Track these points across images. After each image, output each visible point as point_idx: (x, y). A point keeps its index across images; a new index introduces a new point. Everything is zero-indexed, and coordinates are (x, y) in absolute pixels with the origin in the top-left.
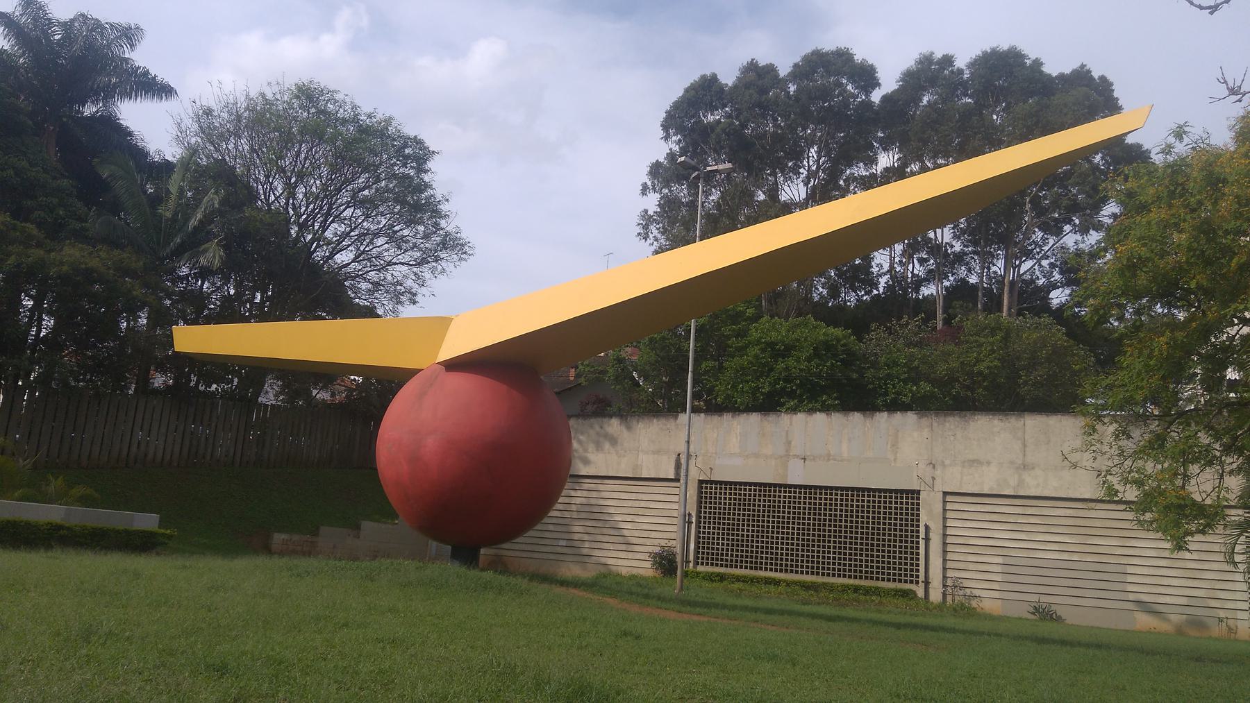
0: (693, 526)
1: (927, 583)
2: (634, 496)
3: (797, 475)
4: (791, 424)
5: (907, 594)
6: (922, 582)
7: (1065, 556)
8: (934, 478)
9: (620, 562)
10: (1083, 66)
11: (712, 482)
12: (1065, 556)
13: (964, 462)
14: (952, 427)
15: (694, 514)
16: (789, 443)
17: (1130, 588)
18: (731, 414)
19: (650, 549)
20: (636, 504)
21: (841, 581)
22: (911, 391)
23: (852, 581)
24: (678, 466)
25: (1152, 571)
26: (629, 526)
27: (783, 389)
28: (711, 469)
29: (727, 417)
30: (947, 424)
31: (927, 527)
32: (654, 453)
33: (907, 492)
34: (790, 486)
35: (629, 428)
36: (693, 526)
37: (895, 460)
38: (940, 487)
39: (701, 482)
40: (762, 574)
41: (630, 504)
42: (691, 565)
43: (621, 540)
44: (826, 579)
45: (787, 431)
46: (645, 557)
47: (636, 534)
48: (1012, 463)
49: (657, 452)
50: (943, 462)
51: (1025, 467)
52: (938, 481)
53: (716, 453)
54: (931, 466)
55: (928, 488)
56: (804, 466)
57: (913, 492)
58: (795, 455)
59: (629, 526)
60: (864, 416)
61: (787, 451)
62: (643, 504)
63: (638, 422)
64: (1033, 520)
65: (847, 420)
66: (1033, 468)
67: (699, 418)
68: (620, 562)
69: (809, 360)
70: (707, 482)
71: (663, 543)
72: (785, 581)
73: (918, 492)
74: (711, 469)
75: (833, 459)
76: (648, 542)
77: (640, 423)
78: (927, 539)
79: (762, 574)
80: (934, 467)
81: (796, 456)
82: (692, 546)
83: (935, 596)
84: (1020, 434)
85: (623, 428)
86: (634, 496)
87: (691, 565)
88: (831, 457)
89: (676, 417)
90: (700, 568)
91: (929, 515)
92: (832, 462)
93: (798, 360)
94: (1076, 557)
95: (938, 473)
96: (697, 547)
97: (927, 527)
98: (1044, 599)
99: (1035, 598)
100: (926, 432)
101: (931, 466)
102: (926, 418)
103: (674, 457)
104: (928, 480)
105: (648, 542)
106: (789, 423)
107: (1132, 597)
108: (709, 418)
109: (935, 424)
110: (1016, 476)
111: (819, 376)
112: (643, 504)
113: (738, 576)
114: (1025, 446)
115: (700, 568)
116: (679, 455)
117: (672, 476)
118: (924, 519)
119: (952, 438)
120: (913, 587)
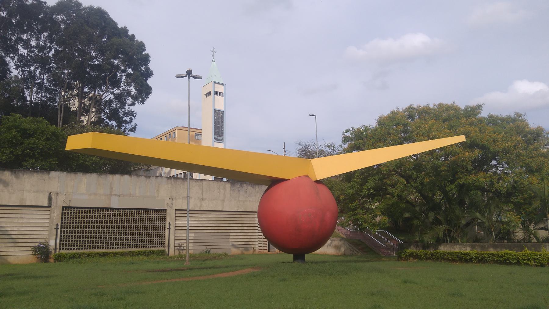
1: (169, 246)
2: (19, 216)
3: (115, 203)
4: (113, 180)
5: (164, 251)
6: (167, 246)
7: (213, 231)
8: (172, 204)
9: (10, 253)
11: (69, 207)
12: (213, 231)
13: (183, 197)
14: (179, 184)
15: (59, 224)
16: (112, 188)
17: (230, 240)
18: (82, 173)
20: (21, 220)
21: (138, 249)
22: (92, 160)
24: (50, 199)
25: (236, 234)
26: (16, 233)
28: (70, 201)
29: (80, 175)
30: (178, 183)
31: (169, 223)
32: (34, 192)
33: (161, 210)
34: (111, 209)
35: (17, 177)
36: (59, 230)
37: (158, 196)
38: (175, 207)
39: (63, 207)
40: (96, 251)
41: (16, 220)
42: (58, 250)
43: (11, 241)
45: (111, 183)
46: (30, 249)
47: (21, 237)
48: (199, 198)
49: (37, 191)
50: (176, 198)
51: (203, 199)
52: (174, 205)
53: (72, 193)
54: (172, 199)
55: (170, 208)
56: (119, 199)
57: (163, 210)
58: (115, 194)
59: (16, 233)
60: (146, 178)
61: (111, 192)
62: (25, 220)
63: (23, 175)
64: (204, 219)
65: (139, 179)
66: (205, 200)
67: (63, 174)
68: (10, 253)
69: (44, 140)
70: (66, 207)
71: (41, 240)
72: (112, 253)
73: (166, 210)
74: (70, 201)
75: (132, 196)
76: (29, 241)
77: (25, 175)
78: (169, 229)
79: (96, 251)
80: (172, 199)
81: (115, 195)
82: (58, 241)
83: (171, 253)
84: (201, 187)
85: (13, 177)
86: (19, 216)
87: (58, 250)
88: (131, 195)
89: (49, 173)
90: (62, 252)
91: (170, 219)
92: (131, 197)
93: (39, 139)
94: (216, 231)
95: (174, 201)
96: (60, 241)
97: (169, 223)
98: (208, 247)
99: (205, 247)
100: (170, 186)
101: (172, 199)
102: (170, 180)
103: (47, 195)
104: (170, 205)
105: (29, 241)
106: (112, 179)
107: (230, 243)
108: (69, 175)
109: (173, 182)
110: (200, 203)
111: (49, 149)
112: (25, 220)
113: (89, 253)
114: (203, 191)
115: (62, 252)
116: (50, 193)
117: (46, 204)
118: (168, 220)
119: (179, 188)
120: (162, 249)
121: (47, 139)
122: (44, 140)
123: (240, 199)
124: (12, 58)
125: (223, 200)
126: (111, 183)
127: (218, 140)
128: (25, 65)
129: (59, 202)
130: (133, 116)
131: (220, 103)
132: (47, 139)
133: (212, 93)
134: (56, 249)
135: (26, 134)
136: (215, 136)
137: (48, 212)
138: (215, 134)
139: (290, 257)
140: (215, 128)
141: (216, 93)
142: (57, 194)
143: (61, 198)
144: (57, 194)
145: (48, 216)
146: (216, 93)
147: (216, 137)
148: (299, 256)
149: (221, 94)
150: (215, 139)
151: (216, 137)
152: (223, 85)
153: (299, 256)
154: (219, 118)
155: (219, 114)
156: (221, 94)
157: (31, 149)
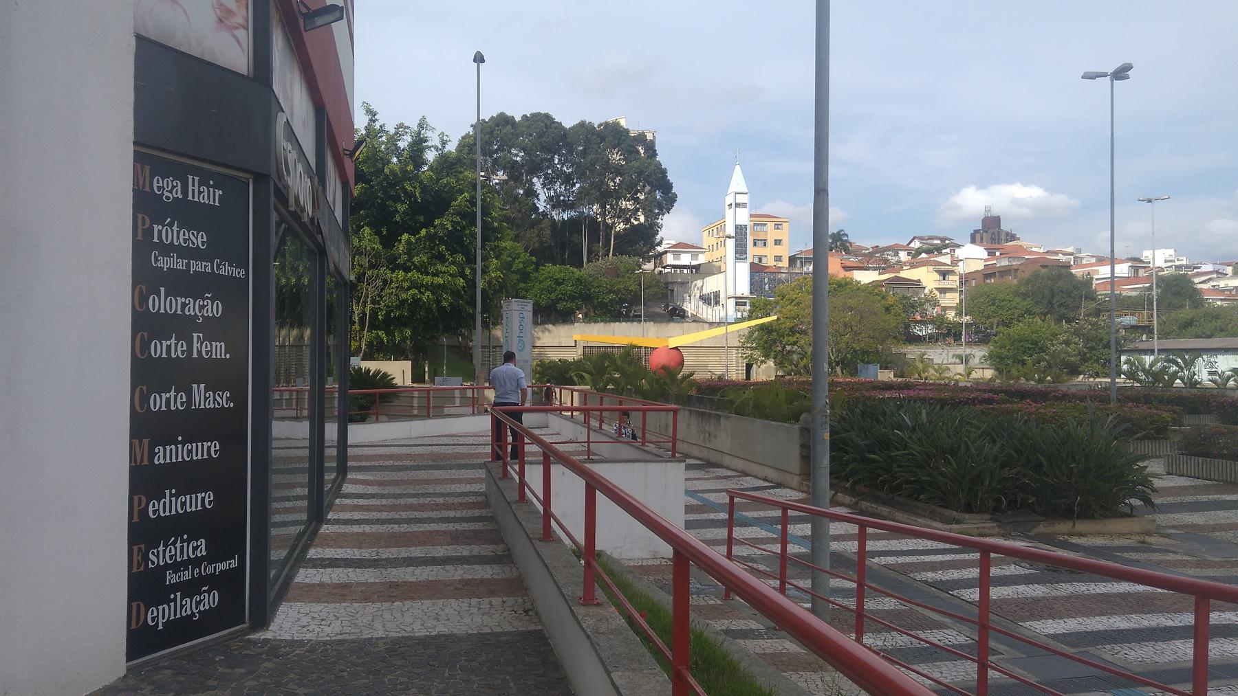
10: (643, 133)
24: (576, 341)
27: (561, 298)
69: (571, 286)
100: (656, 328)
111: (575, 292)
121: (573, 285)
122: (571, 286)
124: (539, 178)
126: (614, 329)
127: (741, 259)
128: (551, 183)
129: (581, 345)
130: (659, 227)
131: (743, 217)
132: (573, 285)
133: (733, 205)
135: (558, 282)
141: (738, 205)
146: (738, 205)
149: (744, 205)
154: (741, 233)
155: (741, 229)
156: (744, 205)
157: (562, 294)
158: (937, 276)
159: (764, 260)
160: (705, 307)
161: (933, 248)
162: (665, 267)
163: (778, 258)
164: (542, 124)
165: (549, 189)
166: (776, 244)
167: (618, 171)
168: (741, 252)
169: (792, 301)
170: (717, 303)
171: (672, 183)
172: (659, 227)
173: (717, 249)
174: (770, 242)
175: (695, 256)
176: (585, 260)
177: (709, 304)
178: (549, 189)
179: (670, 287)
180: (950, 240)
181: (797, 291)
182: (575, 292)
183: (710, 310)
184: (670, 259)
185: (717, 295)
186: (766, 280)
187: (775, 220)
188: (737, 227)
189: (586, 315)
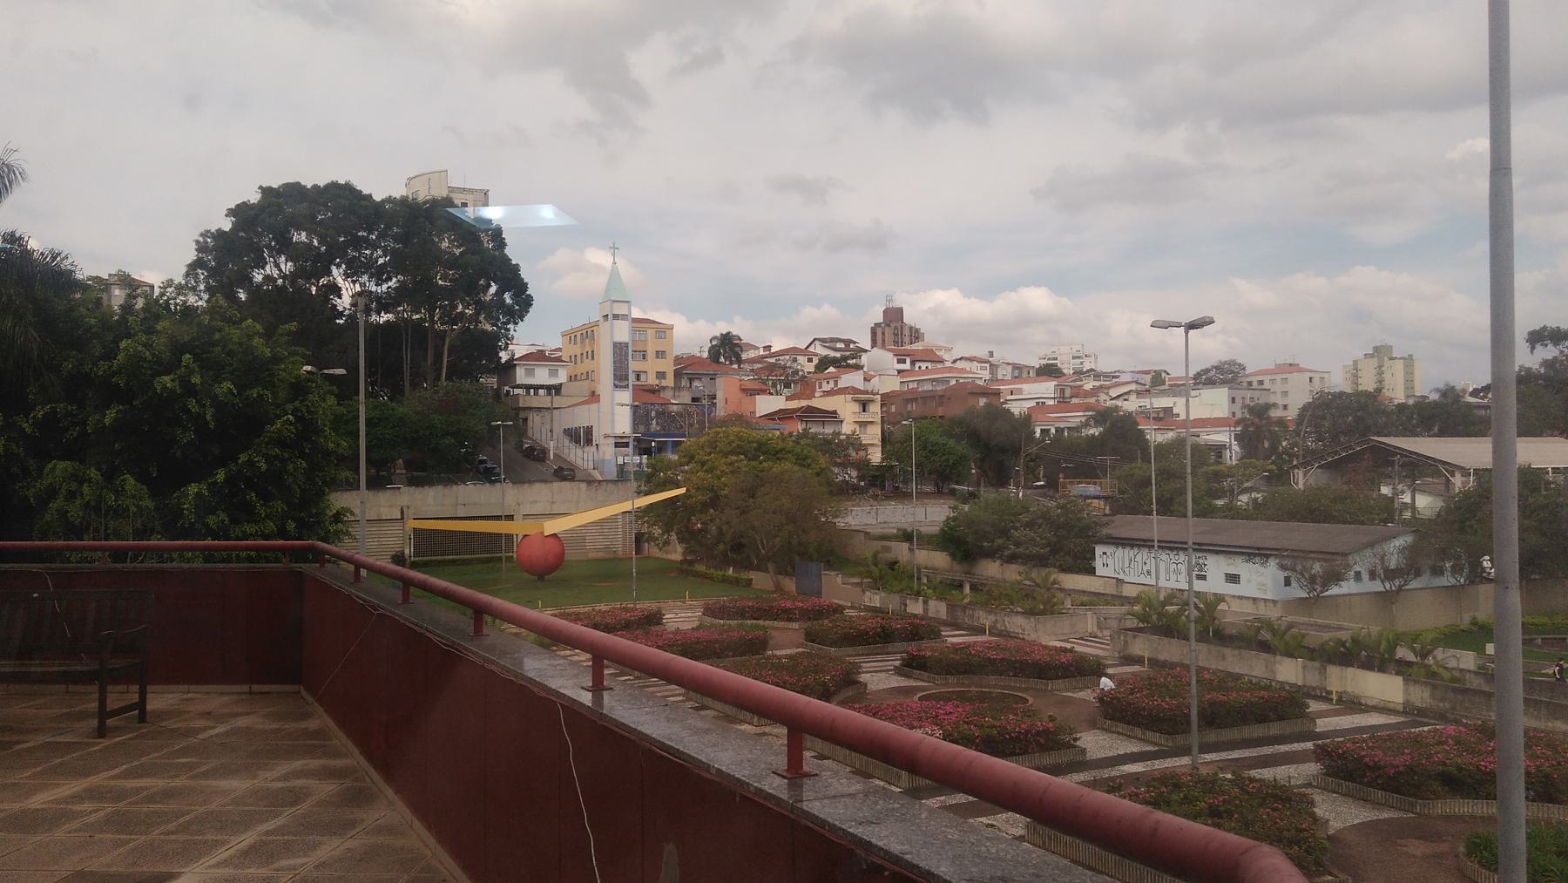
0: (412, 540)
2: (378, 529)
16: (457, 498)
19: (391, 553)
23: (489, 555)
24: (402, 512)
36: (412, 540)
44: (461, 557)
49: (391, 506)
51: (553, 503)
62: (383, 532)
71: (397, 549)
82: (412, 550)
86: (378, 529)
95: (521, 507)
111: (397, 437)
112: (383, 532)
123: (599, 499)
125: (578, 502)
127: (621, 387)
130: (508, 339)
133: (610, 317)
134: (410, 557)
136: (616, 382)
137: (402, 524)
138: (614, 380)
139: (536, 578)
140: (615, 370)
141: (616, 317)
142: (408, 508)
143: (412, 511)
144: (408, 508)
145: (401, 528)
146: (616, 317)
147: (617, 383)
148: (541, 577)
150: (616, 386)
151: (617, 383)
152: (627, 302)
153: (541, 577)
154: (621, 355)
158: (856, 408)
159: (643, 377)
160: (572, 445)
161: (844, 358)
162: (513, 387)
163: (661, 375)
164: (343, 197)
165: (354, 282)
166: (657, 357)
167: (453, 263)
168: (620, 379)
169: (703, 464)
170: (589, 441)
171: (527, 284)
172: (508, 339)
173: (582, 362)
174: (651, 355)
175: (553, 373)
176: (407, 384)
177: (577, 442)
178: (354, 282)
179: (522, 415)
180: (855, 343)
181: (708, 450)
182: (397, 437)
183: (579, 452)
184: (521, 376)
185: (589, 431)
186: (653, 414)
187: (656, 326)
188: (616, 345)
189: (409, 465)
